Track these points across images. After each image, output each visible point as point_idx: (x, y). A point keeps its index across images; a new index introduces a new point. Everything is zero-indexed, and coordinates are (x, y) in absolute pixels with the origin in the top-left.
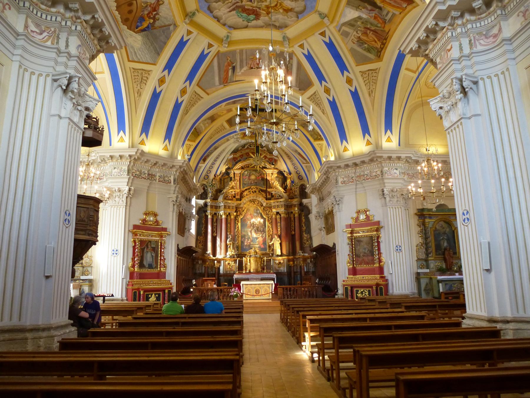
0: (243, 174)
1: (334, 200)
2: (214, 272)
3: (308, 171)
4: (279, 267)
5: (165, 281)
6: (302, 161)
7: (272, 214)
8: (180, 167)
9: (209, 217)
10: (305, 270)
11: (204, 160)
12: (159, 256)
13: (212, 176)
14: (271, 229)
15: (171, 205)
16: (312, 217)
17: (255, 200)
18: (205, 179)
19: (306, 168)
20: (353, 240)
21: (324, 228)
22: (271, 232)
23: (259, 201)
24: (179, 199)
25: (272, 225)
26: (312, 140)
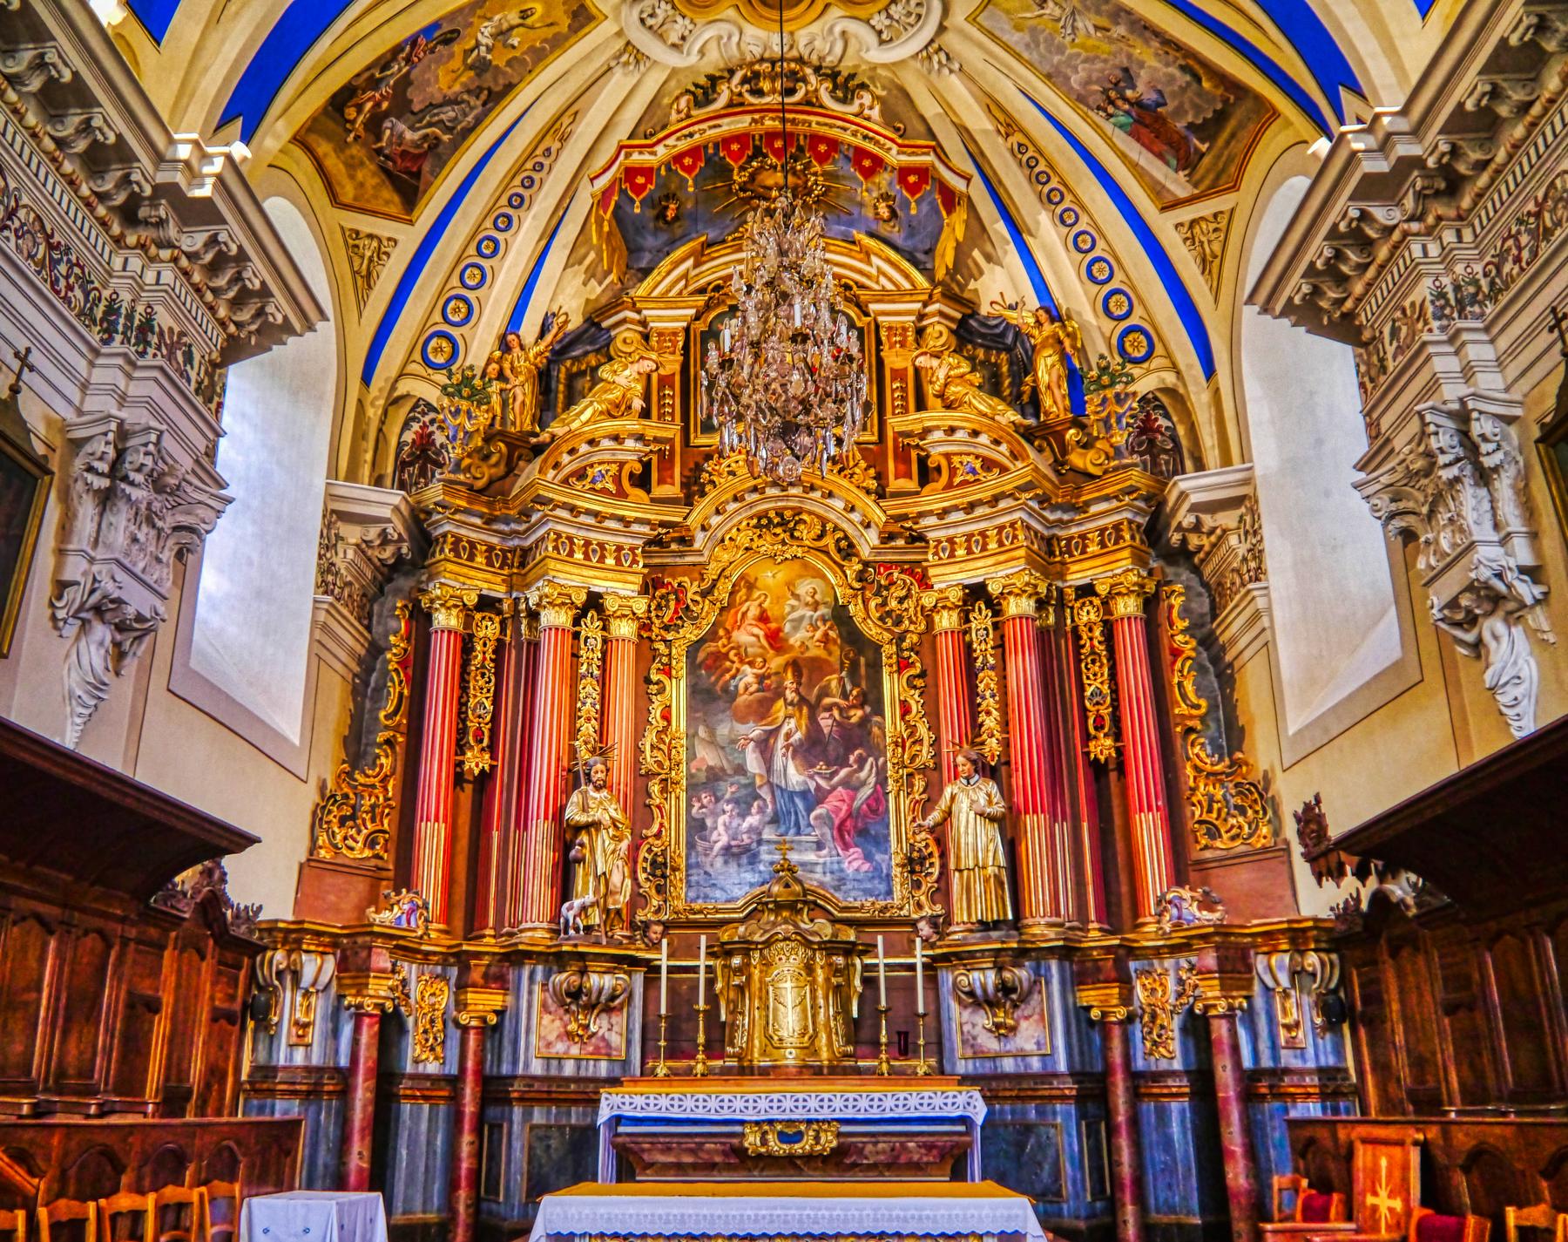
0: (712, 334)
2: (454, 1071)
6: (1156, 190)
7: (928, 600)
9: (446, 619)
13: (479, 345)
14: (923, 730)
17: (798, 511)
18: (427, 362)
22: (925, 754)
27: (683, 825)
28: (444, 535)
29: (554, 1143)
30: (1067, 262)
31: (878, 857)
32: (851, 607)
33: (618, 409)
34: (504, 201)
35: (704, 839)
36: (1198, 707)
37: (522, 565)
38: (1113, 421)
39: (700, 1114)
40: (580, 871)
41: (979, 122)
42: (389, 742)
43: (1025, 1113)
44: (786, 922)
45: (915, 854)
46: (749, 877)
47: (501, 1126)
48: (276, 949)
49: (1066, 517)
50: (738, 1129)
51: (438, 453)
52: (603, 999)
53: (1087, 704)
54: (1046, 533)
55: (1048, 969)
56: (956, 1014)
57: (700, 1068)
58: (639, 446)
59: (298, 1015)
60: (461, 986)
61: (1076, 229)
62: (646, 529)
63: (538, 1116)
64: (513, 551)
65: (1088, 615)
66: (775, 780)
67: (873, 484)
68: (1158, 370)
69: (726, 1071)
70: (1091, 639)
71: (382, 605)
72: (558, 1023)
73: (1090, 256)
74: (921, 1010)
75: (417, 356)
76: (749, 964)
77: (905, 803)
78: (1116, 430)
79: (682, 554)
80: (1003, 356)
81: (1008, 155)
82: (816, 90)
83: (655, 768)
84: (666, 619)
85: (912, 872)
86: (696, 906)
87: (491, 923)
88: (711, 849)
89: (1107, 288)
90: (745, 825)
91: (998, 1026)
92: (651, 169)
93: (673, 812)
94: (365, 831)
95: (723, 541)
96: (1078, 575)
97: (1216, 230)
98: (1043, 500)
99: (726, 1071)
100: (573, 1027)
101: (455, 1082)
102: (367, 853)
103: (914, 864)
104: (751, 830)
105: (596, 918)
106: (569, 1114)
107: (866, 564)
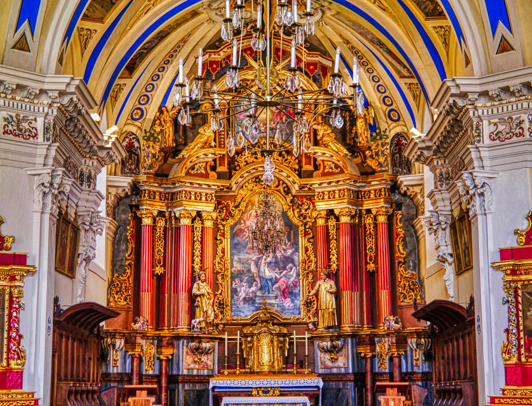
1: (468, 183)
2: (157, 373)
3: (415, 97)
4: (333, 360)
5: (22, 394)
6: (398, 72)
7: (315, 214)
8: (62, 93)
9: (147, 221)
10: (404, 370)
11: (131, 69)
12: (6, 328)
13: (152, 111)
14: (312, 258)
15: (38, 195)
16: (422, 222)
18: (133, 119)
19: (409, 88)
20: (520, 292)
21: (451, 255)
22: (313, 266)
23: (279, 180)
24: (58, 180)
25: (314, 244)
26: (420, 16)
27: (229, 291)
28: (145, 190)
29: (191, 395)
30: (370, 85)
31: (296, 301)
32: (289, 213)
33: (206, 145)
34: (162, 63)
35: (237, 295)
36: (403, 254)
37: (172, 199)
38: (380, 153)
39: (239, 385)
40: (198, 310)
41: (337, 39)
42: (130, 265)
43: (339, 385)
44: (265, 326)
45: (309, 301)
46: (252, 308)
47: (175, 390)
48: (107, 338)
49: (363, 184)
50: (250, 390)
51: (136, 150)
52: (206, 350)
53: (368, 252)
54: (356, 189)
55: (348, 341)
56: (319, 355)
57: (238, 372)
58: (213, 156)
59: (114, 358)
60: (159, 346)
61: (372, 75)
62: (216, 187)
63: (187, 387)
64: (168, 193)
65: (369, 221)
66: (261, 275)
67: (297, 167)
68: (401, 125)
69: (246, 373)
70: (370, 229)
71: (118, 209)
72: (191, 358)
73: (378, 84)
74: (307, 354)
75: (130, 118)
76: (253, 340)
77: (306, 283)
78: (381, 157)
79: (228, 192)
80: (347, 113)
81: (349, 51)
82: (278, 32)
83: (219, 271)
84: (222, 217)
85: (307, 307)
86: (235, 318)
87: (166, 325)
88: (239, 299)
89: (384, 95)
90: (251, 290)
91: (332, 358)
92: (218, 61)
93: (226, 285)
94: (124, 296)
95: (242, 187)
96: (367, 205)
97: (417, 88)
98: (355, 181)
99: (246, 373)
100: (196, 359)
101: (158, 377)
102: (125, 303)
103: (308, 304)
104: (253, 292)
105: (203, 325)
106: (196, 387)
107: (294, 196)
